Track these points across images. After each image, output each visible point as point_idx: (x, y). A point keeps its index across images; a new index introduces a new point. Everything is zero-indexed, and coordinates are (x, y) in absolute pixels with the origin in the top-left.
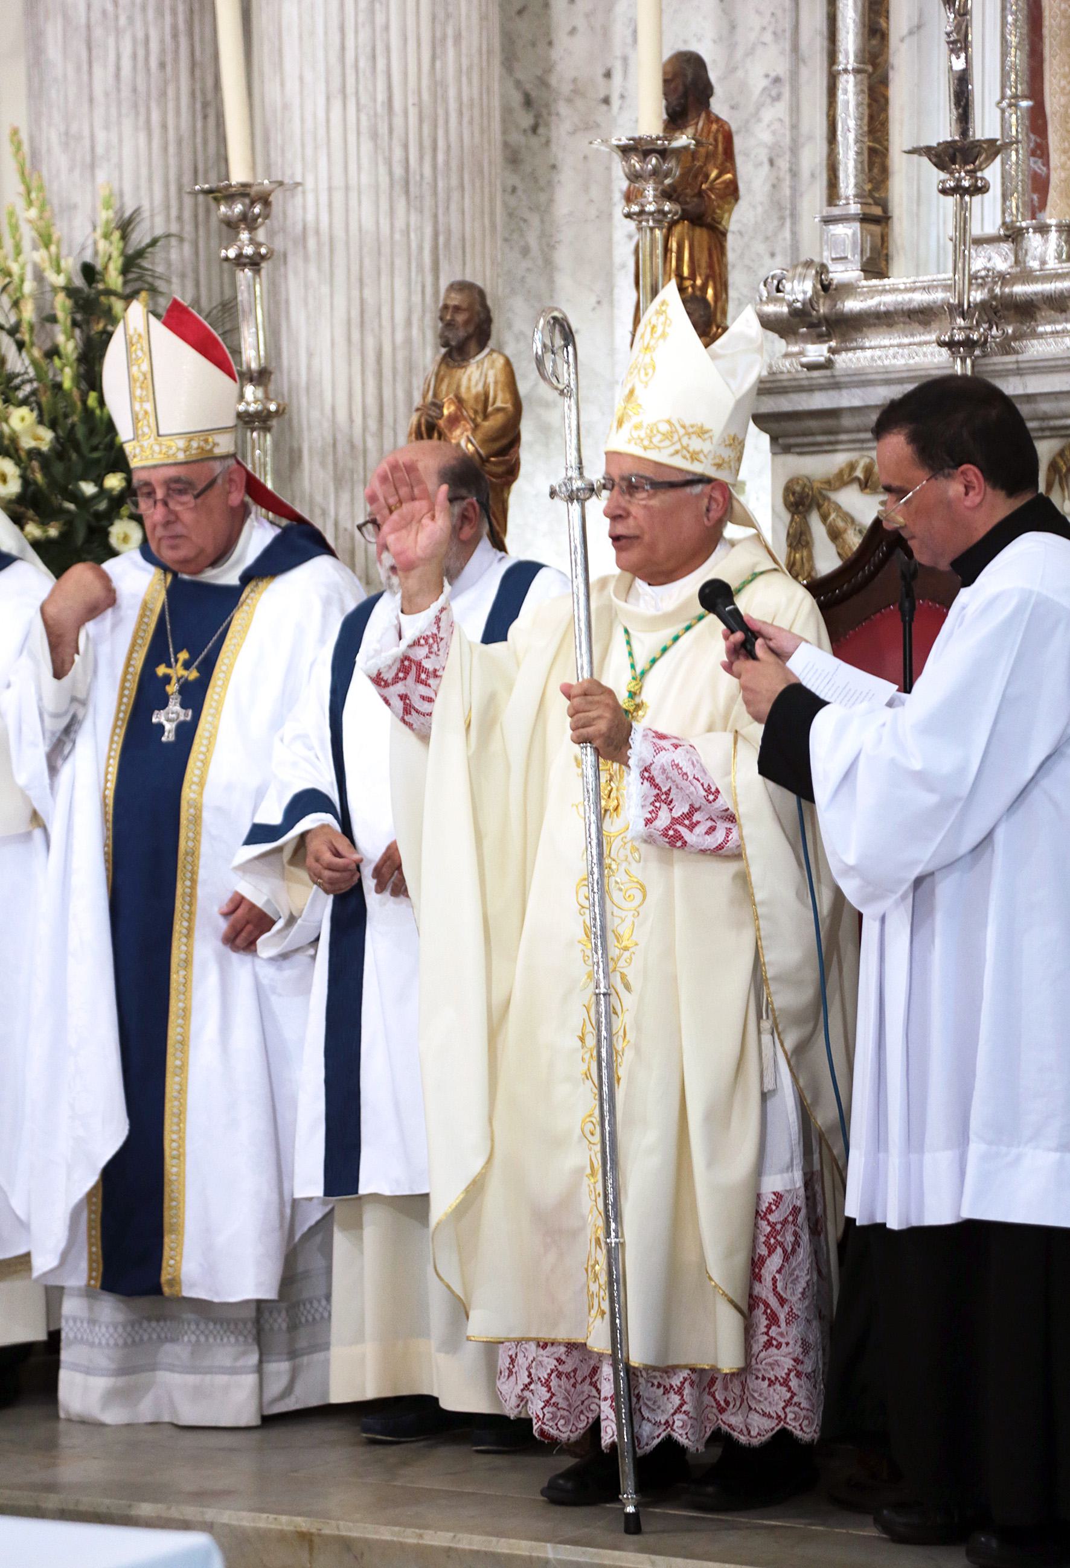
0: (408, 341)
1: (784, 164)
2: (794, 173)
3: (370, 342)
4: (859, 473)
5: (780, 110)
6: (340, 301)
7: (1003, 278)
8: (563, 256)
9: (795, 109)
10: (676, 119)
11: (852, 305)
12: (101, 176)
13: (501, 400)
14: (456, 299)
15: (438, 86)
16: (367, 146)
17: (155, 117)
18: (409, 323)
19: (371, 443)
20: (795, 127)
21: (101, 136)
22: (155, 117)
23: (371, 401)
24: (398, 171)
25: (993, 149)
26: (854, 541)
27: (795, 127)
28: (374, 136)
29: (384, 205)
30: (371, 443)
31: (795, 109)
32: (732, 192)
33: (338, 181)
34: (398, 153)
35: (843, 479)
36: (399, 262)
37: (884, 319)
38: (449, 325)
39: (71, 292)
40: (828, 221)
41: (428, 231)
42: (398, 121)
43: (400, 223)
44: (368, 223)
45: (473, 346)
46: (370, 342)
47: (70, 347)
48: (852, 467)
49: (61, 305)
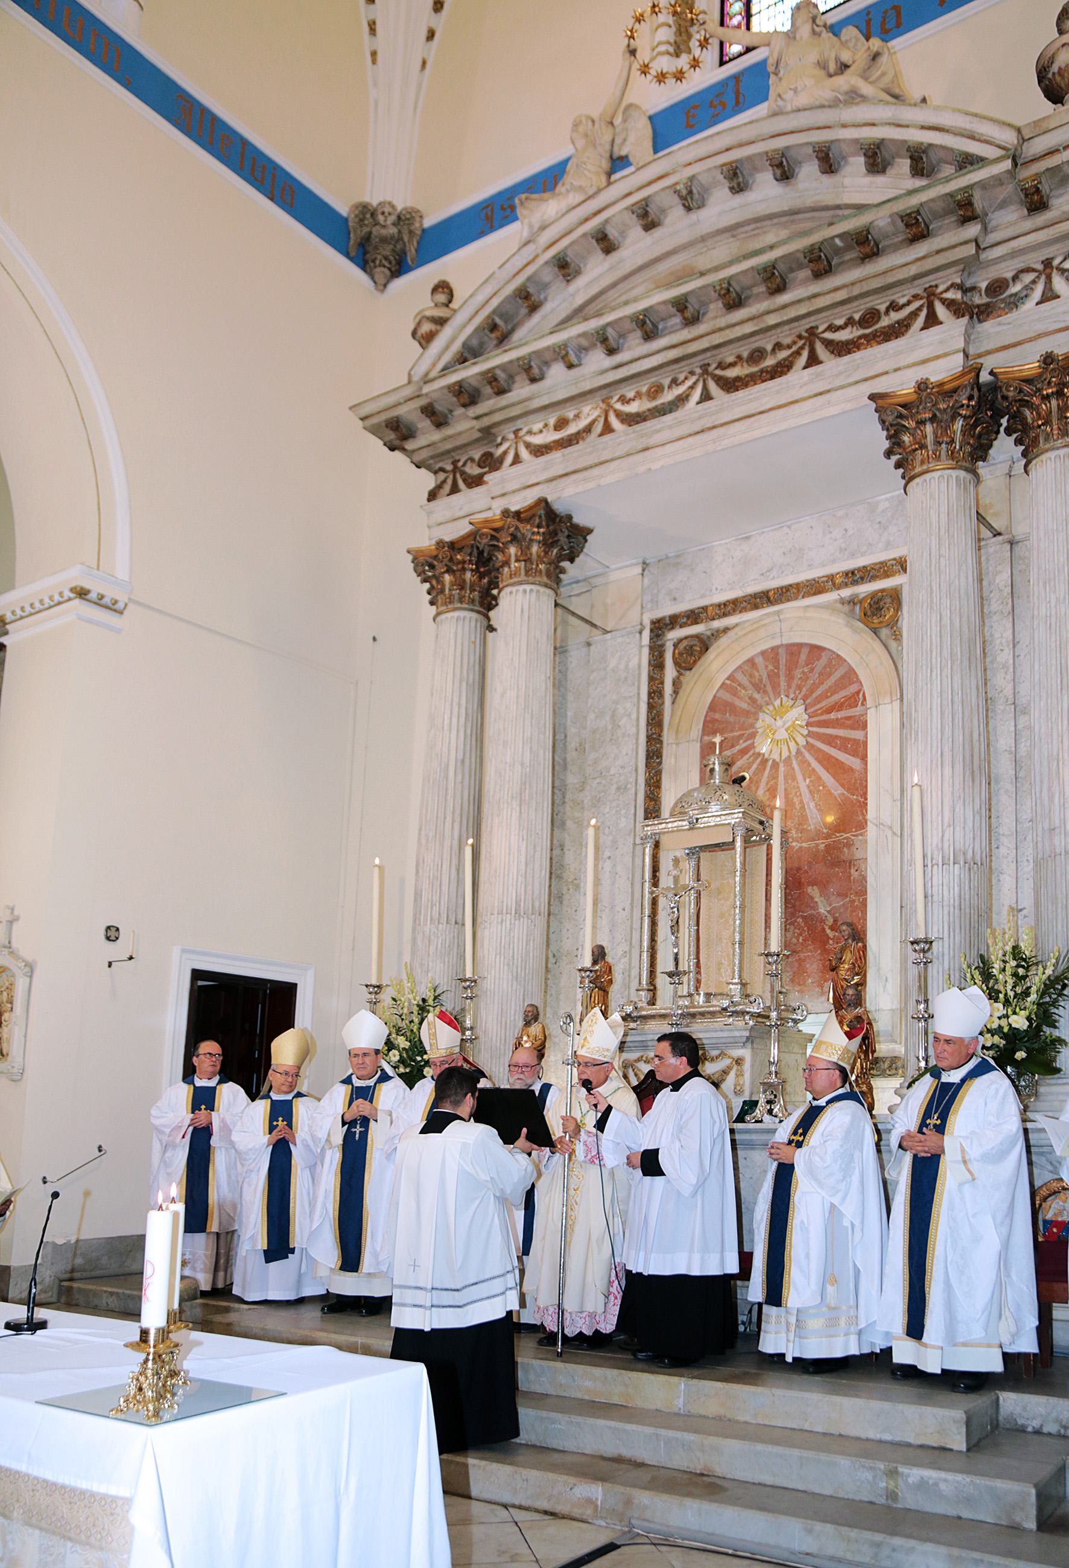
0: (515, 1020)
1: (627, 974)
2: (629, 976)
3: (504, 1020)
4: (644, 1059)
5: (626, 959)
6: (496, 1008)
7: (686, 1007)
8: (562, 997)
9: (630, 959)
10: (595, 962)
11: (644, 1013)
12: (430, 975)
13: (541, 1037)
14: (529, 1009)
15: (527, 952)
16: (506, 968)
17: (446, 959)
18: (515, 1015)
19: (502, 1047)
20: (630, 964)
21: (430, 964)
22: (446, 959)
23: (503, 1035)
24: (515, 974)
25: (685, 973)
26: (642, 1077)
27: (630, 964)
28: (508, 965)
29: (510, 983)
30: (502, 1047)
31: (630, 959)
32: (611, 981)
33: (497, 976)
34: (515, 970)
35: (639, 1060)
36: (514, 999)
37: (653, 1017)
38: (527, 1016)
39: (418, 1005)
40: (637, 990)
41: (522, 990)
42: (515, 962)
43: (514, 988)
44: (505, 987)
45: (533, 1021)
46: (504, 1020)
47: (416, 1021)
48: (642, 1057)
49: (415, 1009)
